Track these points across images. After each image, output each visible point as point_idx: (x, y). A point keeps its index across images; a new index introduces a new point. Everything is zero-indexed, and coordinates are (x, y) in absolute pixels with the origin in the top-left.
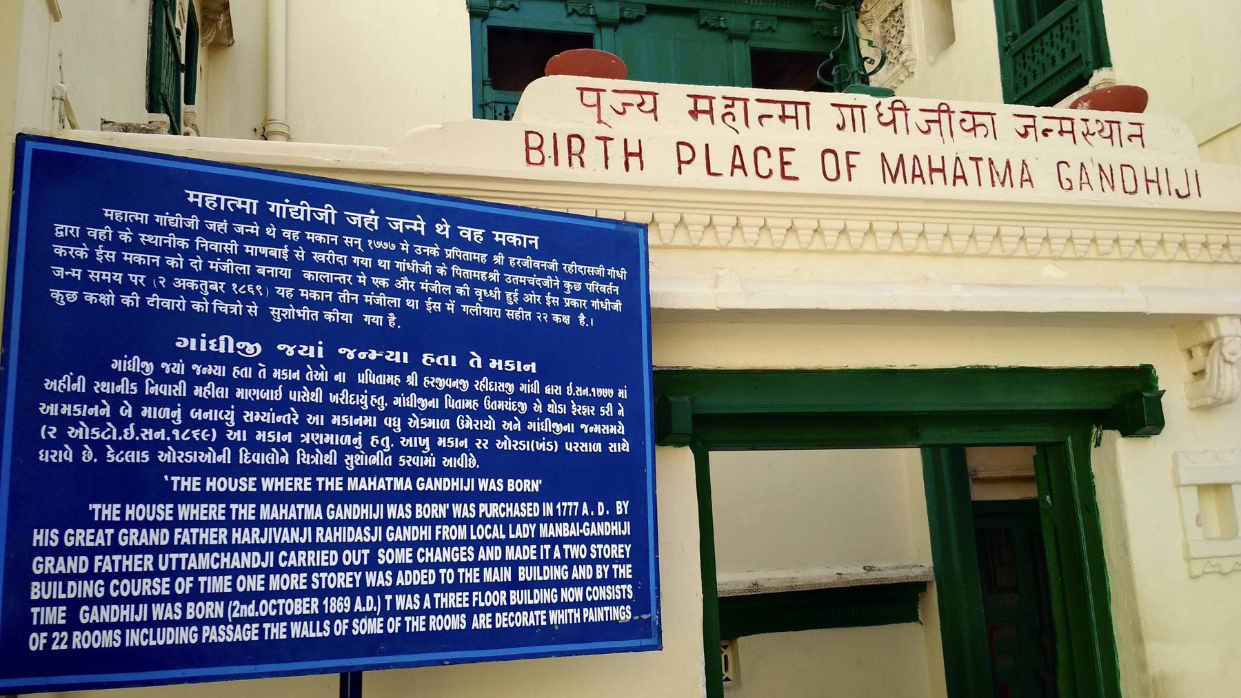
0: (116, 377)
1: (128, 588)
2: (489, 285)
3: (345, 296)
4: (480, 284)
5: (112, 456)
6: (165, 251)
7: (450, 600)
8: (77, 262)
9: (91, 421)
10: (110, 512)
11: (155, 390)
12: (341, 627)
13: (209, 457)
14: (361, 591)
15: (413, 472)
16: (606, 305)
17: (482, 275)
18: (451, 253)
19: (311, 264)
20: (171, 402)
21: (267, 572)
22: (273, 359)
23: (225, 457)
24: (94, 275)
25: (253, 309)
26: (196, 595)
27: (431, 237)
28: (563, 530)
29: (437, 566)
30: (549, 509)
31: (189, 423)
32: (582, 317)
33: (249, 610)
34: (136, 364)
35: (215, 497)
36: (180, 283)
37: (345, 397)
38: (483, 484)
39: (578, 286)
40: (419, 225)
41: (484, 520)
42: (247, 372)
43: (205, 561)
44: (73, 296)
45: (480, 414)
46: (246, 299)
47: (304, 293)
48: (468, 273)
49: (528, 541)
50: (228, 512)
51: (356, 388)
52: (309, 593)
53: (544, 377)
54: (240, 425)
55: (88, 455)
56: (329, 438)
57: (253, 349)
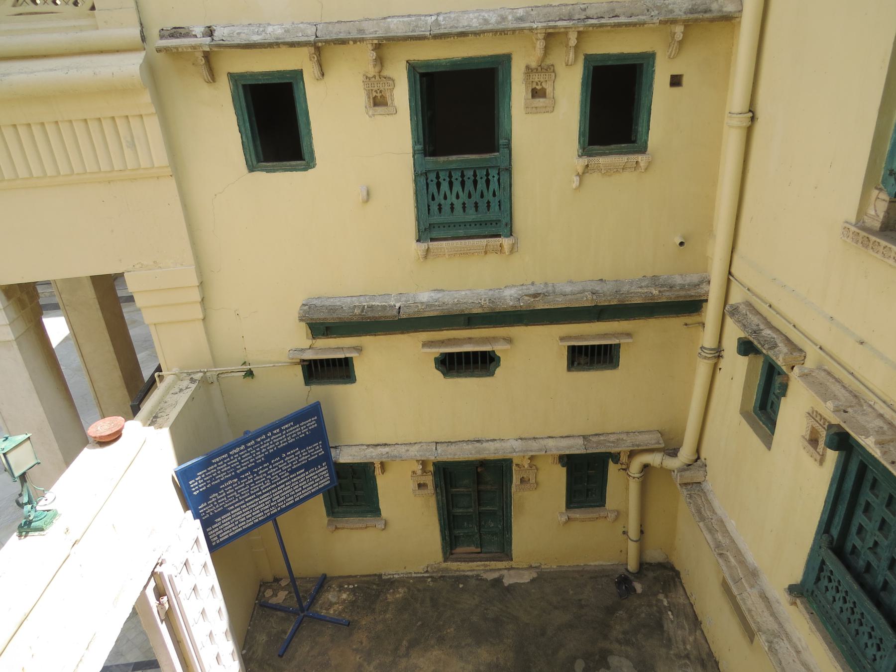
0: (211, 499)
1: (226, 528)
2: (283, 439)
3: (251, 461)
4: (280, 440)
5: (216, 511)
6: (212, 474)
7: (289, 499)
8: (196, 486)
9: (210, 508)
10: (219, 519)
11: (219, 497)
12: (269, 514)
13: (234, 501)
14: (271, 507)
15: (275, 483)
16: (313, 427)
17: (281, 438)
18: (272, 438)
19: (242, 459)
20: (223, 497)
21: (251, 513)
22: (240, 479)
23: (237, 500)
24: (200, 486)
25: (233, 473)
26: (239, 523)
27: (267, 437)
28: (312, 475)
29: (285, 495)
30: (307, 473)
31: (227, 499)
32: (307, 433)
33: (250, 520)
34: (214, 495)
35: (237, 507)
36: (217, 477)
37: (257, 478)
38: (291, 477)
39: (305, 427)
40: (264, 437)
41: (293, 482)
42: (236, 484)
43: (239, 517)
44: (198, 492)
45: (288, 464)
46: (231, 472)
47: (243, 465)
48: (278, 440)
49: (304, 481)
50: (241, 508)
51: (258, 475)
52: (261, 512)
53: (300, 450)
54: (238, 493)
55: (211, 514)
56: (256, 486)
57: (236, 480)
